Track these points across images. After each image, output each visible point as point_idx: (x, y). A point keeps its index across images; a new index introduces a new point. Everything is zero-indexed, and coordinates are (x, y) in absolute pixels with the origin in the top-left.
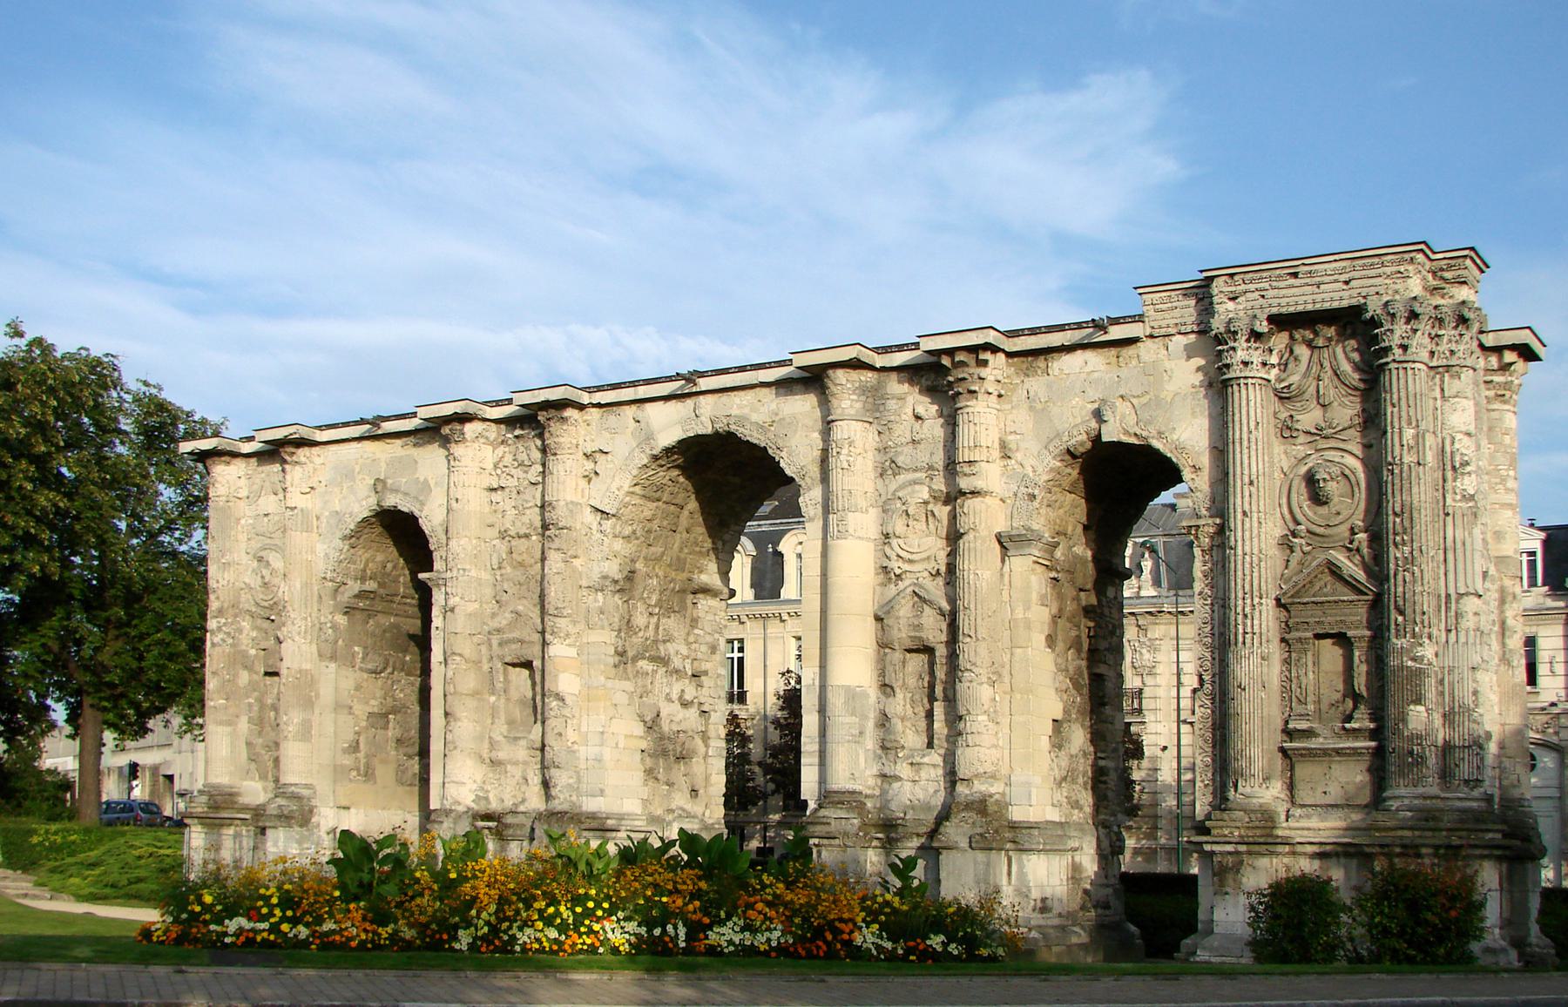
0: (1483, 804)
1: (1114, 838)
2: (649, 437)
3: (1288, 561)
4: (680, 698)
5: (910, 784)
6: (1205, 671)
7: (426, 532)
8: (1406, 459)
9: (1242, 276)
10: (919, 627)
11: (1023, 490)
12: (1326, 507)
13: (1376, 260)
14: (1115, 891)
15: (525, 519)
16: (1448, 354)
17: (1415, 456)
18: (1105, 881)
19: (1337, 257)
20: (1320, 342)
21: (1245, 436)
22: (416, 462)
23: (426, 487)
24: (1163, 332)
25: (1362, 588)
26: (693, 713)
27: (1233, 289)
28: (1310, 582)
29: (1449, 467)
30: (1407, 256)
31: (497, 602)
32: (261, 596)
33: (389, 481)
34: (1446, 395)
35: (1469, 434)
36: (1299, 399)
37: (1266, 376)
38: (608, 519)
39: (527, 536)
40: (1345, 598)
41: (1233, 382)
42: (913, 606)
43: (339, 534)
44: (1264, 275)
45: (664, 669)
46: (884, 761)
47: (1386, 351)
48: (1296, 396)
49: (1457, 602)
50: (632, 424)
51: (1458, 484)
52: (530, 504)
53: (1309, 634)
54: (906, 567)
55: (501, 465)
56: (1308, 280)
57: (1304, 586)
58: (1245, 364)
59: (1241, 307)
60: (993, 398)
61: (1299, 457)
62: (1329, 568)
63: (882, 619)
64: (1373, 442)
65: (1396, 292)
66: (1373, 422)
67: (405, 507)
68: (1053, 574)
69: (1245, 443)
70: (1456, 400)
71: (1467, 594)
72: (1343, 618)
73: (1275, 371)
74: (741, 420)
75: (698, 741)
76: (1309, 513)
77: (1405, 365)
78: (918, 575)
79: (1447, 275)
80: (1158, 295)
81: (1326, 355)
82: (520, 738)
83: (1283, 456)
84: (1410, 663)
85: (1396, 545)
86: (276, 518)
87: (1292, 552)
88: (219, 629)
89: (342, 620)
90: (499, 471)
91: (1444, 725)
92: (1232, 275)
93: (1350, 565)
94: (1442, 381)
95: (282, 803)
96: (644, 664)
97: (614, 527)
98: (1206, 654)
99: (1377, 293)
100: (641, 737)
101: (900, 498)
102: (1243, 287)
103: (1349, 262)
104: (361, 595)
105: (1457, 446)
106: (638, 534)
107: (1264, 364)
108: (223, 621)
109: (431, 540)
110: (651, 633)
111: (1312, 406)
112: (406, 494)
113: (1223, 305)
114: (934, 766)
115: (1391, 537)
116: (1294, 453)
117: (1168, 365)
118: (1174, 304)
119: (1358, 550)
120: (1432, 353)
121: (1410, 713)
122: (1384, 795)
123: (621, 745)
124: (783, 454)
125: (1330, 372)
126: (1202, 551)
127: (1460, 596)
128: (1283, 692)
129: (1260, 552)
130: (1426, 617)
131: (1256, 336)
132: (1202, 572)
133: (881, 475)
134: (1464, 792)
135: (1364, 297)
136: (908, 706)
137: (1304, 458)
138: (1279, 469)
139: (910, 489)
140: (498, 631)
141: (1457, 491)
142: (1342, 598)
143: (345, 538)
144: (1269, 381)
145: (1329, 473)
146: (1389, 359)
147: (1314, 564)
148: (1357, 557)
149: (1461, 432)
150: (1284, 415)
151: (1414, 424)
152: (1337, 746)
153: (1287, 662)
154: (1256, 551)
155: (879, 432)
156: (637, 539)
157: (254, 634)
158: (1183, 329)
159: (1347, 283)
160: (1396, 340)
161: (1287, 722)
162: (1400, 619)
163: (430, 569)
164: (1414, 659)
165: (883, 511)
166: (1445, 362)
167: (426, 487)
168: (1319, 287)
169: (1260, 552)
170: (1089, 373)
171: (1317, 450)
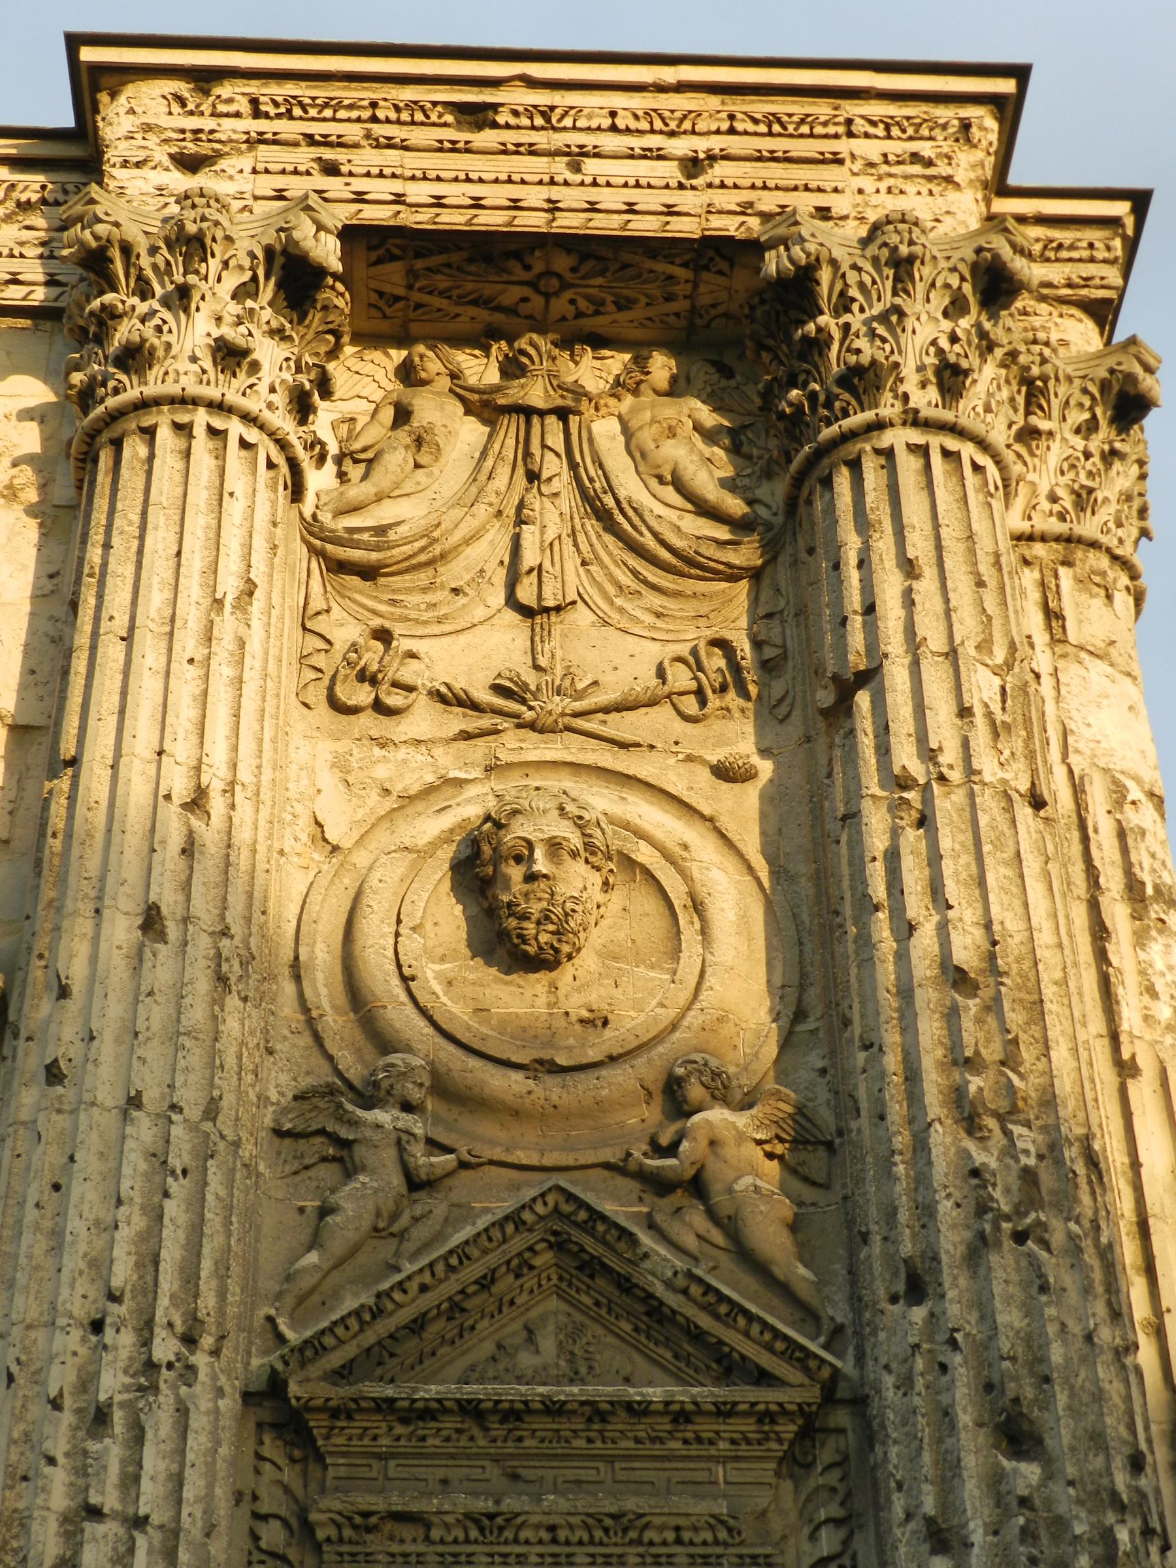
3: (325, 1211)
8: (987, 765)
9: (253, 87)
12: (538, 982)
13: (822, 108)
17: (1021, 765)
19: (669, 75)
21: (192, 614)
27: (208, 123)
28: (455, 1308)
29: (1112, 880)
30: (944, 113)
34: (1072, 636)
35: (1158, 801)
36: (423, 577)
40: (655, 1394)
41: (162, 420)
56: (541, 139)
57: (417, 1326)
61: (412, 782)
62: (559, 1244)
69: (188, 643)
72: (631, 1504)
77: (952, 444)
81: (556, 440)
83: (328, 780)
87: (350, 1171)
99: (823, 213)
103: (713, 102)
113: (145, 171)
115: (933, 1083)
116: (381, 772)
125: (569, 499)
129: (212, 1111)
137: (429, 791)
138: (305, 821)
142: (634, 1393)
145: (579, 823)
146: (888, 408)
148: (697, 1219)
151: (1000, 655)
154: (191, 1096)
159: (693, 165)
166: (1054, 526)
168: (576, 168)
169: (212, 1111)
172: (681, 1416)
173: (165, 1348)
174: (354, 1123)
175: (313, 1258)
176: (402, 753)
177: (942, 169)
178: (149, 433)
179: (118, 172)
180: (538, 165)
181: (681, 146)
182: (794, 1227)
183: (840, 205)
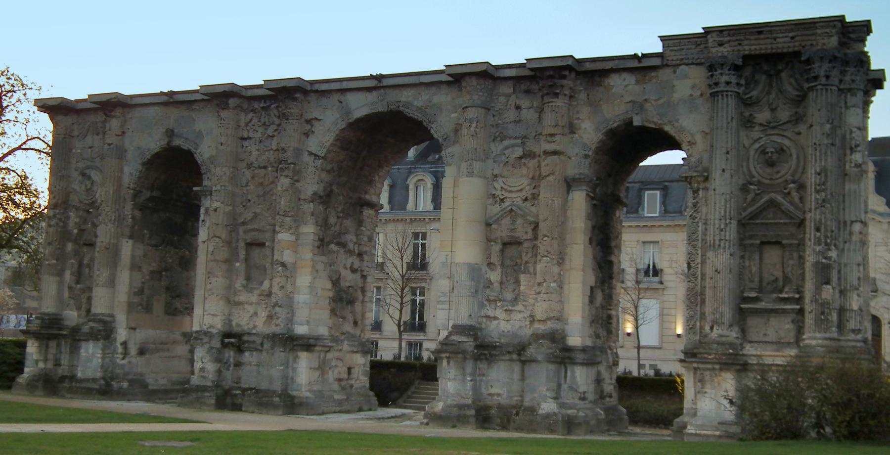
0: (862, 344)
1: (615, 356)
2: (349, 113)
3: (746, 199)
4: (351, 267)
5: (503, 321)
6: (693, 261)
7: (199, 162)
10: (513, 230)
11: (583, 152)
13: (812, 25)
14: (615, 387)
15: (264, 157)
16: (851, 82)
18: (610, 382)
20: (772, 72)
22: (194, 120)
23: (200, 135)
24: (674, 63)
25: (793, 216)
26: (357, 276)
27: (721, 39)
29: (848, 147)
30: (832, 24)
31: (244, 206)
32: (84, 197)
33: (176, 131)
37: (738, 91)
38: (319, 159)
39: (265, 167)
40: (782, 221)
42: (511, 218)
43: (140, 162)
44: (742, 31)
45: (344, 250)
46: (488, 307)
47: (816, 78)
48: (755, 103)
49: (851, 226)
50: (337, 104)
51: (853, 157)
52: (268, 149)
53: (758, 242)
54: (507, 195)
55: (250, 125)
58: (728, 83)
59: (725, 50)
60: (567, 98)
63: (491, 225)
64: (802, 131)
65: (824, 44)
66: (802, 120)
67: (185, 146)
68: (595, 202)
70: (854, 109)
71: (856, 221)
72: (780, 233)
73: (743, 88)
74: (407, 105)
75: (359, 293)
76: (760, 171)
77: (827, 87)
78: (514, 200)
79: (852, 36)
80: (673, 41)
82: (255, 288)
83: (745, 138)
84: (824, 261)
85: (817, 192)
86: (97, 150)
87: (749, 194)
88: (54, 216)
89: (138, 213)
90: (248, 128)
91: (840, 297)
92: (721, 31)
93: (784, 202)
94: (846, 97)
95: (93, 325)
96: (333, 247)
97: (322, 164)
98: (693, 251)
100: (330, 290)
101: (504, 154)
102: (728, 38)
104: (151, 199)
105: (853, 135)
106: (335, 169)
107: (738, 84)
108: (58, 211)
109: (202, 167)
110: (338, 227)
111: (765, 109)
112: (186, 139)
114: (520, 312)
116: (752, 136)
117: (676, 83)
118: (682, 47)
119: (789, 193)
120: (841, 81)
121: (823, 289)
122: (804, 337)
123: (319, 294)
124: (433, 126)
126: (693, 191)
127: (852, 222)
128: (740, 275)
130: (833, 234)
131: (736, 68)
132: (693, 203)
133: (494, 140)
134: (852, 336)
135: (804, 47)
136: (504, 276)
139: (511, 149)
140: (244, 223)
141: (853, 161)
143: (143, 164)
144: (738, 93)
147: (763, 201)
149: (856, 127)
150: (747, 114)
151: (830, 121)
152: (774, 308)
153: (742, 257)
155: (494, 116)
156: (334, 172)
157: (77, 220)
158: (686, 61)
159: (792, 38)
160: (822, 73)
161: (742, 292)
162: (818, 234)
163: (200, 185)
164: (826, 258)
165: (494, 162)
166: (848, 86)
167: (200, 135)
170: (626, 86)
171: (767, 135)
172: (785, 224)
173: (728, 221)
174: (748, 187)
175: (745, 205)
176: (755, 133)
177: (831, 34)
178: (718, 96)
179: (712, 49)
180: (769, 41)
181: (791, 35)
182: (801, 199)
183: (814, 43)
